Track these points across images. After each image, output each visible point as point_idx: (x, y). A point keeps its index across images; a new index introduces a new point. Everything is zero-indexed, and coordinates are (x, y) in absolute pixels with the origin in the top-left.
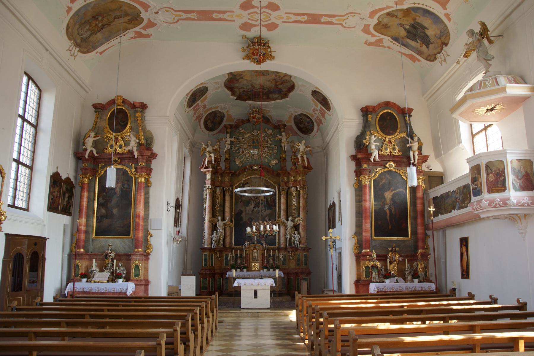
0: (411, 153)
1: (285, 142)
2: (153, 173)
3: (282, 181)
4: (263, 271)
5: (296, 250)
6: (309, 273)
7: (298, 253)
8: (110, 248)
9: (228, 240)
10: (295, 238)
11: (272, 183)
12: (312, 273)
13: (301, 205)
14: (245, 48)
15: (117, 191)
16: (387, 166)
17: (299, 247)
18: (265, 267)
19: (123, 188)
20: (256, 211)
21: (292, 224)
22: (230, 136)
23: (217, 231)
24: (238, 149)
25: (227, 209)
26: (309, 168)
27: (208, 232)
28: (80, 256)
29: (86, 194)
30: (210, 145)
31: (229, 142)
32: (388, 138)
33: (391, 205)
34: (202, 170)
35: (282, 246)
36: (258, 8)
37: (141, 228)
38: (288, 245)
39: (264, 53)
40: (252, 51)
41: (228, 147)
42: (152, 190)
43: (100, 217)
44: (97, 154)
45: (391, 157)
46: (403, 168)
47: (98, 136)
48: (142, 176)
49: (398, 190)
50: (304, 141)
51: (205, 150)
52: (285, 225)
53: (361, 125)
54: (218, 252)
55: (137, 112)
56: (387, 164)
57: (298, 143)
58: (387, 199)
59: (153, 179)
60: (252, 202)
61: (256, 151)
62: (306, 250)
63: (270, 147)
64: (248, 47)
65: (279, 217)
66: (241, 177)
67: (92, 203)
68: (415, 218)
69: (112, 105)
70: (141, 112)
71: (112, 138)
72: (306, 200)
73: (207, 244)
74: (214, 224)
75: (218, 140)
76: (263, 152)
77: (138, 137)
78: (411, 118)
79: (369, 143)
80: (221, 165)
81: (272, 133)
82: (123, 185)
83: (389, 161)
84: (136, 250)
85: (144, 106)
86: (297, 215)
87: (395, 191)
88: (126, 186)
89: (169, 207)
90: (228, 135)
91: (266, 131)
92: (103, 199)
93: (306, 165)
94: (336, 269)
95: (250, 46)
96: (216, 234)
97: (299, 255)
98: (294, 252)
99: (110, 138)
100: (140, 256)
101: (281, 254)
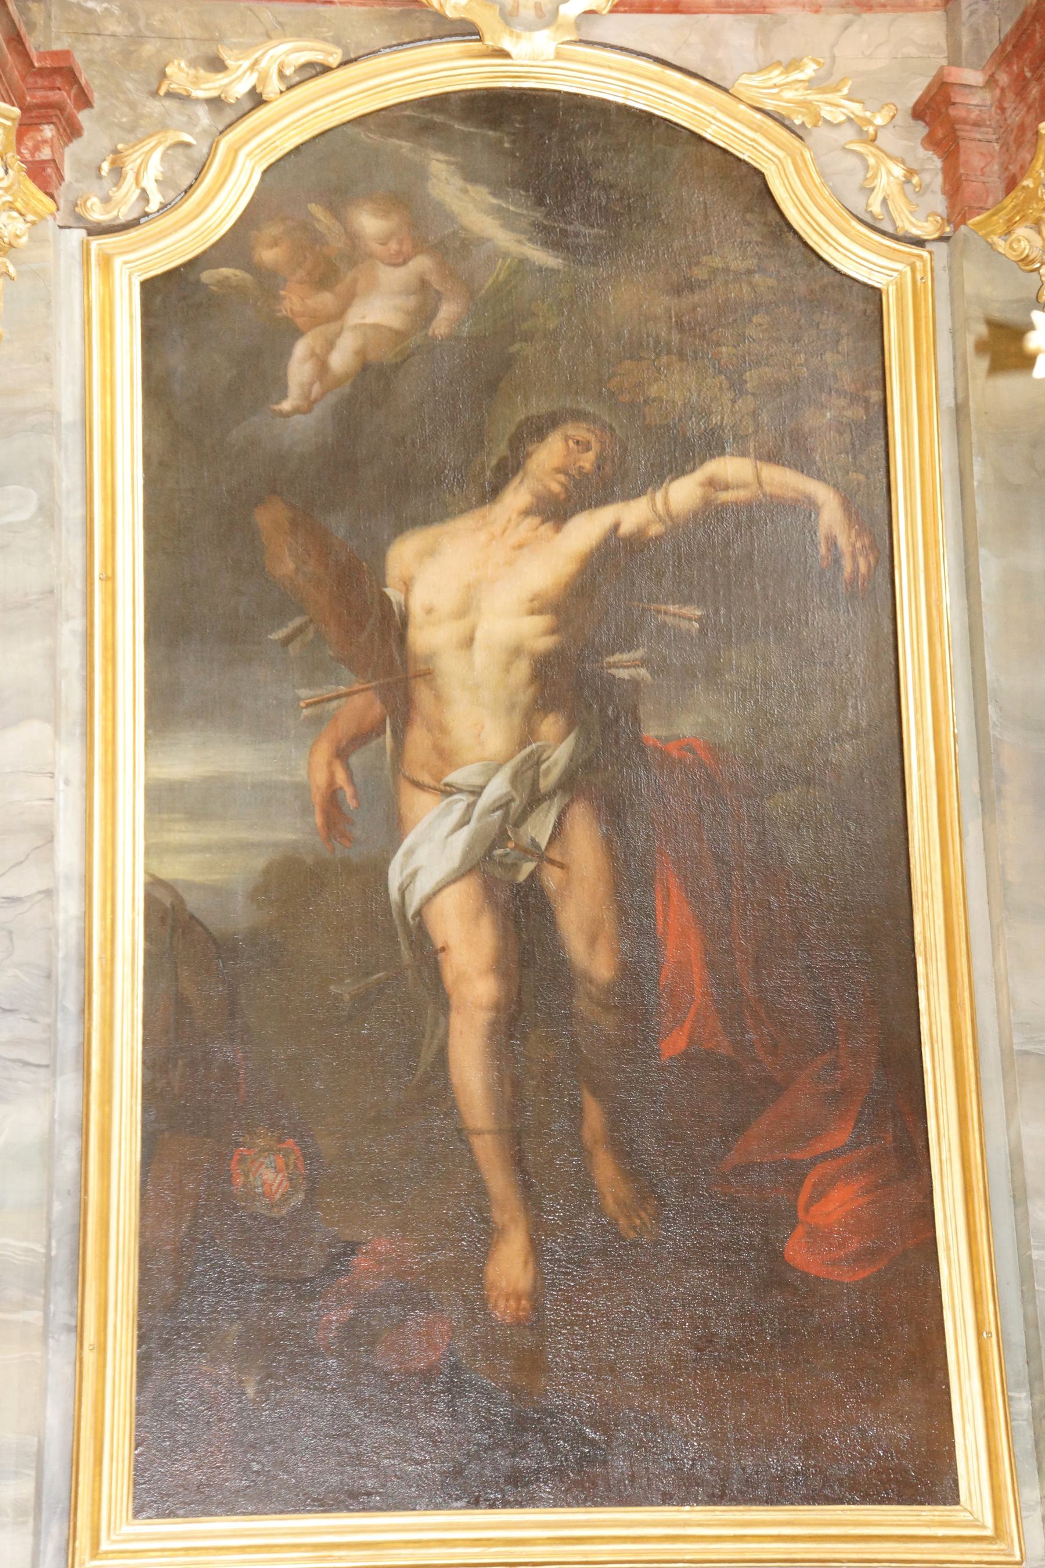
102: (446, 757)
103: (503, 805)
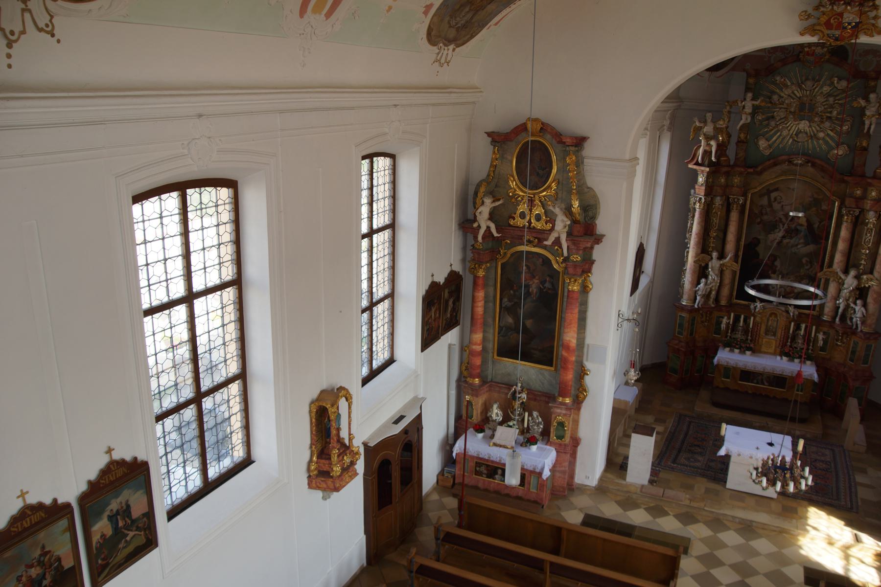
4: (782, 359)
5: (851, 331)
8: (519, 385)
9: (725, 292)
10: (855, 312)
11: (828, 194)
15: (532, 291)
17: (859, 329)
18: (787, 355)
19: (541, 286)
20: (787, 243)
21: (855, 283)
23: (706, 277)
24: (768, 119)
25: (731, 237)
27: (690, 279)
28: (475, 392)
29: (481, 294)
30: (709, 120)
31: (748, 110)
34: (690, 166)
35: (825, 318)
38: (837, 320)
41: (747, 119)
42: (592, 296)
43: (504, 328)
44: (498, 232)
47: (499, 200)
48: (575, 280)
52: (840, 281)
54: (704, 314)
55: (567, 153)
59: (596, 277)
61: (804, 125)
65: (830, 265)
67: (491, 304)
69: (522, 133)
71: (522, 200)
74: (703, 265)
75: (728, 102)
76: (821, 128)
77: (568, 211)
82: (543, 282)
84: (561, 399)
85: (580, 142)
88: (547, 285)
90: (750, 95)
92: (509, 300)
96: (706, 284)
97: (856, 344)
99: (519, 198)
100: (566, 410)
101: (822, 333)
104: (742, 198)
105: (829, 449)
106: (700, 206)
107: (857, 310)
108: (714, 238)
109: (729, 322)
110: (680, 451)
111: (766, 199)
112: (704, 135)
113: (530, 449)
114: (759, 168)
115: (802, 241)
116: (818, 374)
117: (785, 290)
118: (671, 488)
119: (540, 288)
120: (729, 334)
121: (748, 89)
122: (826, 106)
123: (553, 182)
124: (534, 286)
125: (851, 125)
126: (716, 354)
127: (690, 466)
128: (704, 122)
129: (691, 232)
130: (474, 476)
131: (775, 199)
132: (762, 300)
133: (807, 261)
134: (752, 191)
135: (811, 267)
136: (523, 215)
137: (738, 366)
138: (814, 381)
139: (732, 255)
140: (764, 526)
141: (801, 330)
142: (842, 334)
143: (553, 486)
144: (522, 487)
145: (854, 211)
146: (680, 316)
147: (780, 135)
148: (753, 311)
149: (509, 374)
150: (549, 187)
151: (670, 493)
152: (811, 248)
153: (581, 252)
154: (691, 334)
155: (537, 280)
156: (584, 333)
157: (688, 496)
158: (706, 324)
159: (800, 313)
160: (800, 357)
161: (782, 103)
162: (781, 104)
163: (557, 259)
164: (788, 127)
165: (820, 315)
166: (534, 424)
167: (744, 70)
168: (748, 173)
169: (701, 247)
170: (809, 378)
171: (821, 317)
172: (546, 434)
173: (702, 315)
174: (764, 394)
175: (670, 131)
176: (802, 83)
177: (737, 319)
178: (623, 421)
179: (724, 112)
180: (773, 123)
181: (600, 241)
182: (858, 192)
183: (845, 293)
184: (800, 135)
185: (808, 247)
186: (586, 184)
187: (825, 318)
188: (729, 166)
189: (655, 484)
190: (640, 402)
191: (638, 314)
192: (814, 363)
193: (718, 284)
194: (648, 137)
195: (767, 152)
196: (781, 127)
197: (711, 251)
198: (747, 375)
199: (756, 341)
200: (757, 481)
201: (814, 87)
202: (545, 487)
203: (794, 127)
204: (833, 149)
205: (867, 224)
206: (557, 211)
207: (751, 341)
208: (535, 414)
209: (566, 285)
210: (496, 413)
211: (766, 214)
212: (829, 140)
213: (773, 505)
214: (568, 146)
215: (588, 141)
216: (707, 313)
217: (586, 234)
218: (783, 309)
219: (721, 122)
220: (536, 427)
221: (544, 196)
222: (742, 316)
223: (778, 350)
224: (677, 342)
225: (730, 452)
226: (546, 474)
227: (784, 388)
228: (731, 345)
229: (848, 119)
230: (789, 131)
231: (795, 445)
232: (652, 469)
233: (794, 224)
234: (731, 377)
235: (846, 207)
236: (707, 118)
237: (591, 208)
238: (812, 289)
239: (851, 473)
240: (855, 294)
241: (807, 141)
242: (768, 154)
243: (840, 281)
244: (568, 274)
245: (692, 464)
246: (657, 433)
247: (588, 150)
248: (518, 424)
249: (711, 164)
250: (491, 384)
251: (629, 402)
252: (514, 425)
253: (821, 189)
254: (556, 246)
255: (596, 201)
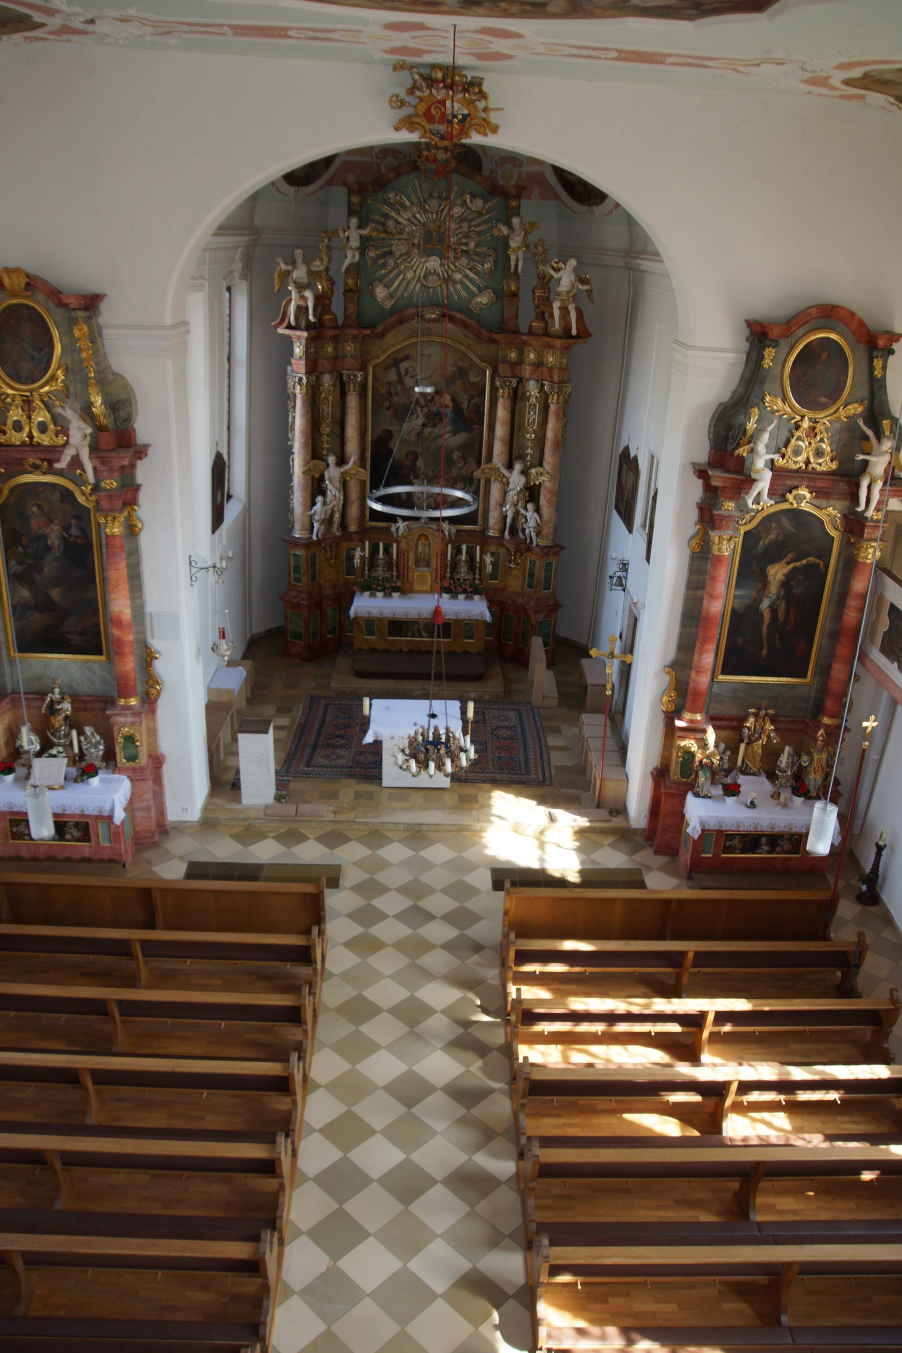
0: (865, 483)
1: (519, 248)
2: (143, 496)
3: (505, 361)
5: (525, 547)
6: (554, 607)
7: (530, 557)
8: (57, 690)
10: (526, 520)
12: (561, 606)
13: (550, 434)
14: (403, 95)
15: (53, 543)
16: (790, 497)
18: (447, 590)
19: (65, 534)
20: (430, 434)
21: (523, 480)
22: (360, 220)
23: (323, 493)
25: (352, 431)
26: (584, 334)
27: (301, 499)
30: (299, 260)
31: (355, 243)
32: (810, 420)
33: (778, 598)
34: (281, 331)
35: (491, 533)
36: (446, 31)
37: (127, 650)
38: (506, 533)
39: (462, 115)
40: (422, 108)
41: (354, 257)
42: (145, 541)
45: (806, 475)
46: (833, 502)
48: (114, 519)
49: (804, 561)
50: (573, 263)
51: (286, 275)
52: (504, 480)
53: (740, 370)
55: (73, 322)
56: (790, 493)
57: (556, 263)
58: (772, 582)
60: (419, 409)
61: (433, 263)
62: (551, 553)
63: (476, 253)
64: (411, 92)
65: (489, 459)
66: (390, 338)
68: (835, 635)
70: (88, 320)
71: (13, 401)
72: (563, 415)
73: (301, 530)
74: (317, 476)
75: (325, 232)
76: (456, 267)
77: (87, 413)
78: (891, 358)
79: (752, 450)
80: (333, 307)
81: (484, 208)
82: (67, 528)
83: (796, 487)
84: (122, 702)
86: (537, 456)
87: (798, 564)
88: (74, 531)
89: (194, 570)
90: (354, 221)
91: (465, 202)
92: (20, 563)
93: (574, 332)
94: (621, 637)
95: (420, 90)
96: (324, 503)
97: (533, 563)
98: (522, 554)
99: (9, 400)
100: (134, 717)
101: (489, 555)
102: (769, 593)
103: (775, 599)
104: (361, 373)
105: (514, 709)
106: (301, 389)
107: (528, 517)
108: (328, 436)
109: (364, 555)
110: (315, 748)
111: (394, 370)
112: (295, 282)
113: (88, 784)
114: (380, 328)
115: (448, 428)
116: (490, 612)
117: (435, 500)
118: (307, 802)
119: (64, 537)
120: (366, 572)
121: (351, 212)
122: (460, 236)
123: (57, 370)
124: (53, 535)
125: (494, 262)
126: (351, 603)
127: (331, 767)
128: (292, 264)
129: (294, 429)
130: (11, 841)
131: (407, 372)
132: (405, 519)
133: (459, 457)
134: (373, 363)
135: (465, 464)
136: (17, 426)
137: (384, 616)
138: (486, 621)
139: (356, 457)
140: (437, 828)
141: (462, 554)
142: (515, 552)
143: (136, 833)
144: (87, 842)
145: (511, 382)
146: (294, 554)
147: (404, 279)
148: (395, 535)
149: (39, 678)
150: (54, 378)
151: (305, 808)
152: (462, 437)
153: (116, 474)
154: (314, 579)
155: (57, 525)
156: (141, 596)
157: (331, 808)
158: (333, 561)
159: (458, 531)
160: (465, 591)
161: (401, 232)
162: (399, 233)
163: (82, 490)
164: (412, 267)
165: (484, 530)
166: (89, 745)
167: (344, 184)
168: (365, 336)
169: (310, 451)
170: (480, 619)
171: (486, 532)
172: (109, 757)
173: (325, 549)
174: (423, 650)
175: (246, 279)
176: (425, 202)
177: (374, 550)
178: (228, 719)
179: (321, 247)
180: (391, 262)
181: (143, 455)
182: (513, 355)
183: (512, 496)
184: (430, 278)
185: (457, 436)
186: (110, 367)
187: (491, 533)
188: (336, 327)
189: (283, 800)
190: (252, 688)
191: (229, 560)
192: (484, 597)
193: (342, 502)
194: (206, 289)
195: (388, 305)
196: (403, 267)
197: (326, 455)
198: (397, 626)
199: (406, 578)
200: (404, 767)
201: (442, 207)
202: (121, 836)
203: (420, 267)
204: (475, 295)
205: (528, 399)
206: (69, 413)
207: (398, 577)
208: (88, 730)
209: (102, 527)
210: (28, 740)
211: (397, 394)
212: (468, 284)
213: (447, 797)
214: (74, 310)
215: (105, 300)
216: (331, 546)
217: (120, 446)
218: (435, 527)
219: (317, 263)
220: (93, 750)
221: (47, 393)
222: (381, 545)
223: (437, 586)
224: (294, 593)
225: (379, 735)
226: (119, 816)
227: (450, 638)
228: (370, 587)
229: (491, 253)
230: (415, 272)
231: (464, 711)
232: (277, 780)
233: (434, 406)
234: (376, 633)
235: (499, 376)
236: (296, 257)
237: (123, 405)
238: (459, 494)
239: (542, 737)
240: (524, 496)
241: (441, 286)
242: (389, 307)
243: (504, 480)
244: (102, 510)
245: (333, 763)
246: (275, 728)
247: (107, 314)
248: (65, 751)
249: (309, 327)
250: (13, 698)
251: (234, 690)
252: (59, 752)
253: (466, 355)
254: (76, 470)
255: (128, 394)
